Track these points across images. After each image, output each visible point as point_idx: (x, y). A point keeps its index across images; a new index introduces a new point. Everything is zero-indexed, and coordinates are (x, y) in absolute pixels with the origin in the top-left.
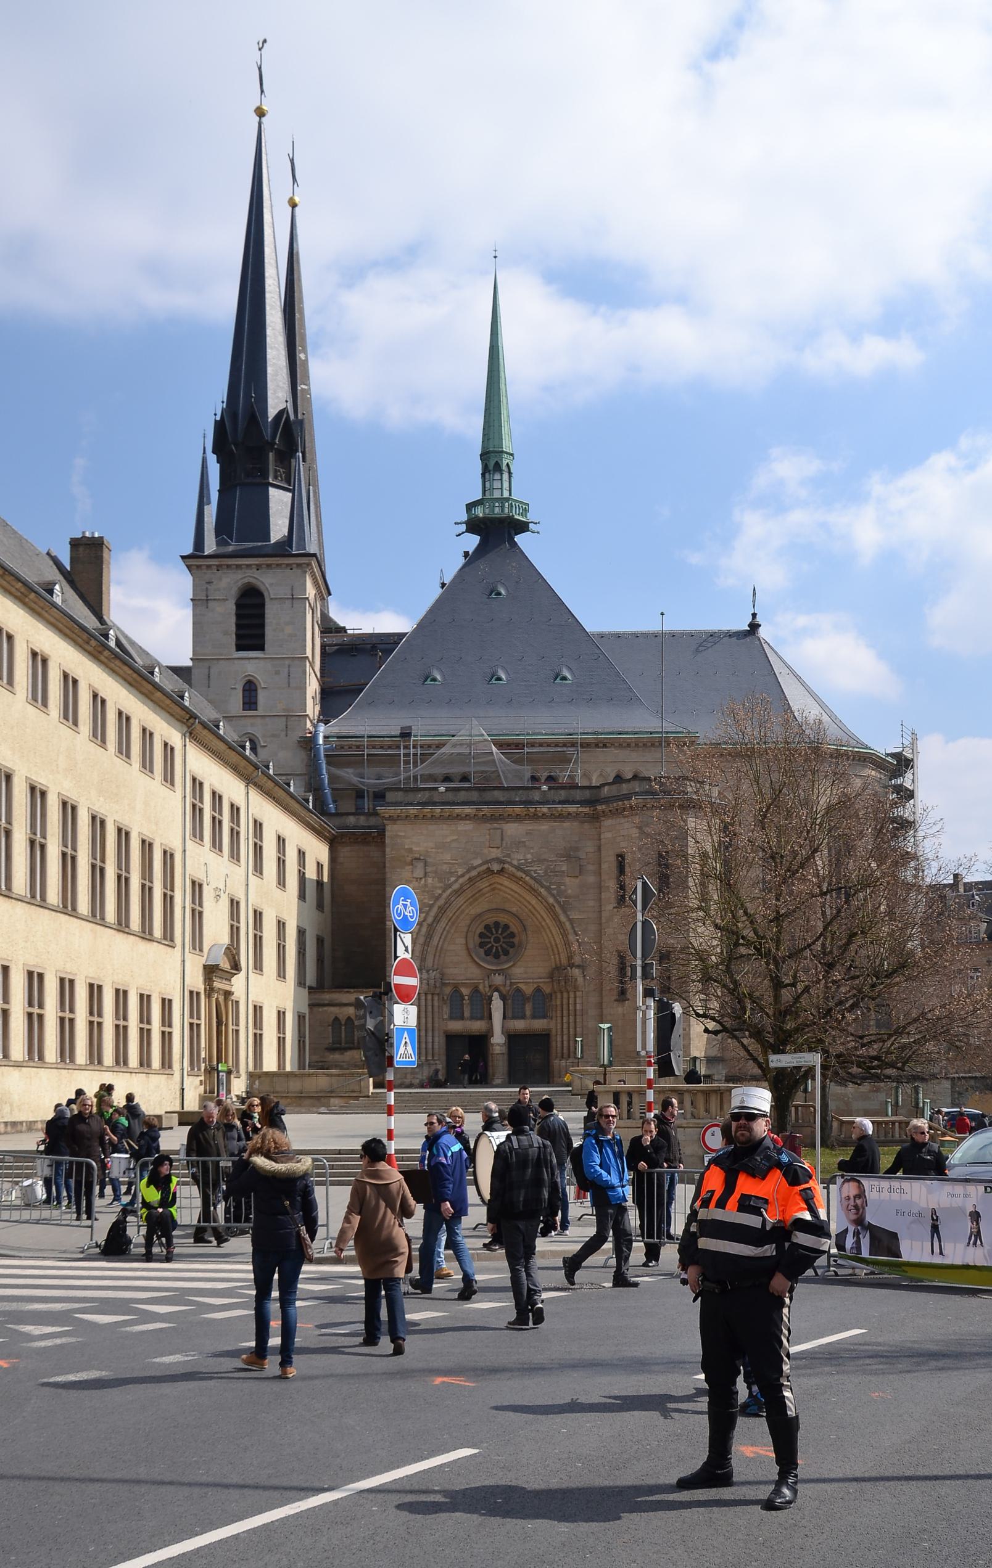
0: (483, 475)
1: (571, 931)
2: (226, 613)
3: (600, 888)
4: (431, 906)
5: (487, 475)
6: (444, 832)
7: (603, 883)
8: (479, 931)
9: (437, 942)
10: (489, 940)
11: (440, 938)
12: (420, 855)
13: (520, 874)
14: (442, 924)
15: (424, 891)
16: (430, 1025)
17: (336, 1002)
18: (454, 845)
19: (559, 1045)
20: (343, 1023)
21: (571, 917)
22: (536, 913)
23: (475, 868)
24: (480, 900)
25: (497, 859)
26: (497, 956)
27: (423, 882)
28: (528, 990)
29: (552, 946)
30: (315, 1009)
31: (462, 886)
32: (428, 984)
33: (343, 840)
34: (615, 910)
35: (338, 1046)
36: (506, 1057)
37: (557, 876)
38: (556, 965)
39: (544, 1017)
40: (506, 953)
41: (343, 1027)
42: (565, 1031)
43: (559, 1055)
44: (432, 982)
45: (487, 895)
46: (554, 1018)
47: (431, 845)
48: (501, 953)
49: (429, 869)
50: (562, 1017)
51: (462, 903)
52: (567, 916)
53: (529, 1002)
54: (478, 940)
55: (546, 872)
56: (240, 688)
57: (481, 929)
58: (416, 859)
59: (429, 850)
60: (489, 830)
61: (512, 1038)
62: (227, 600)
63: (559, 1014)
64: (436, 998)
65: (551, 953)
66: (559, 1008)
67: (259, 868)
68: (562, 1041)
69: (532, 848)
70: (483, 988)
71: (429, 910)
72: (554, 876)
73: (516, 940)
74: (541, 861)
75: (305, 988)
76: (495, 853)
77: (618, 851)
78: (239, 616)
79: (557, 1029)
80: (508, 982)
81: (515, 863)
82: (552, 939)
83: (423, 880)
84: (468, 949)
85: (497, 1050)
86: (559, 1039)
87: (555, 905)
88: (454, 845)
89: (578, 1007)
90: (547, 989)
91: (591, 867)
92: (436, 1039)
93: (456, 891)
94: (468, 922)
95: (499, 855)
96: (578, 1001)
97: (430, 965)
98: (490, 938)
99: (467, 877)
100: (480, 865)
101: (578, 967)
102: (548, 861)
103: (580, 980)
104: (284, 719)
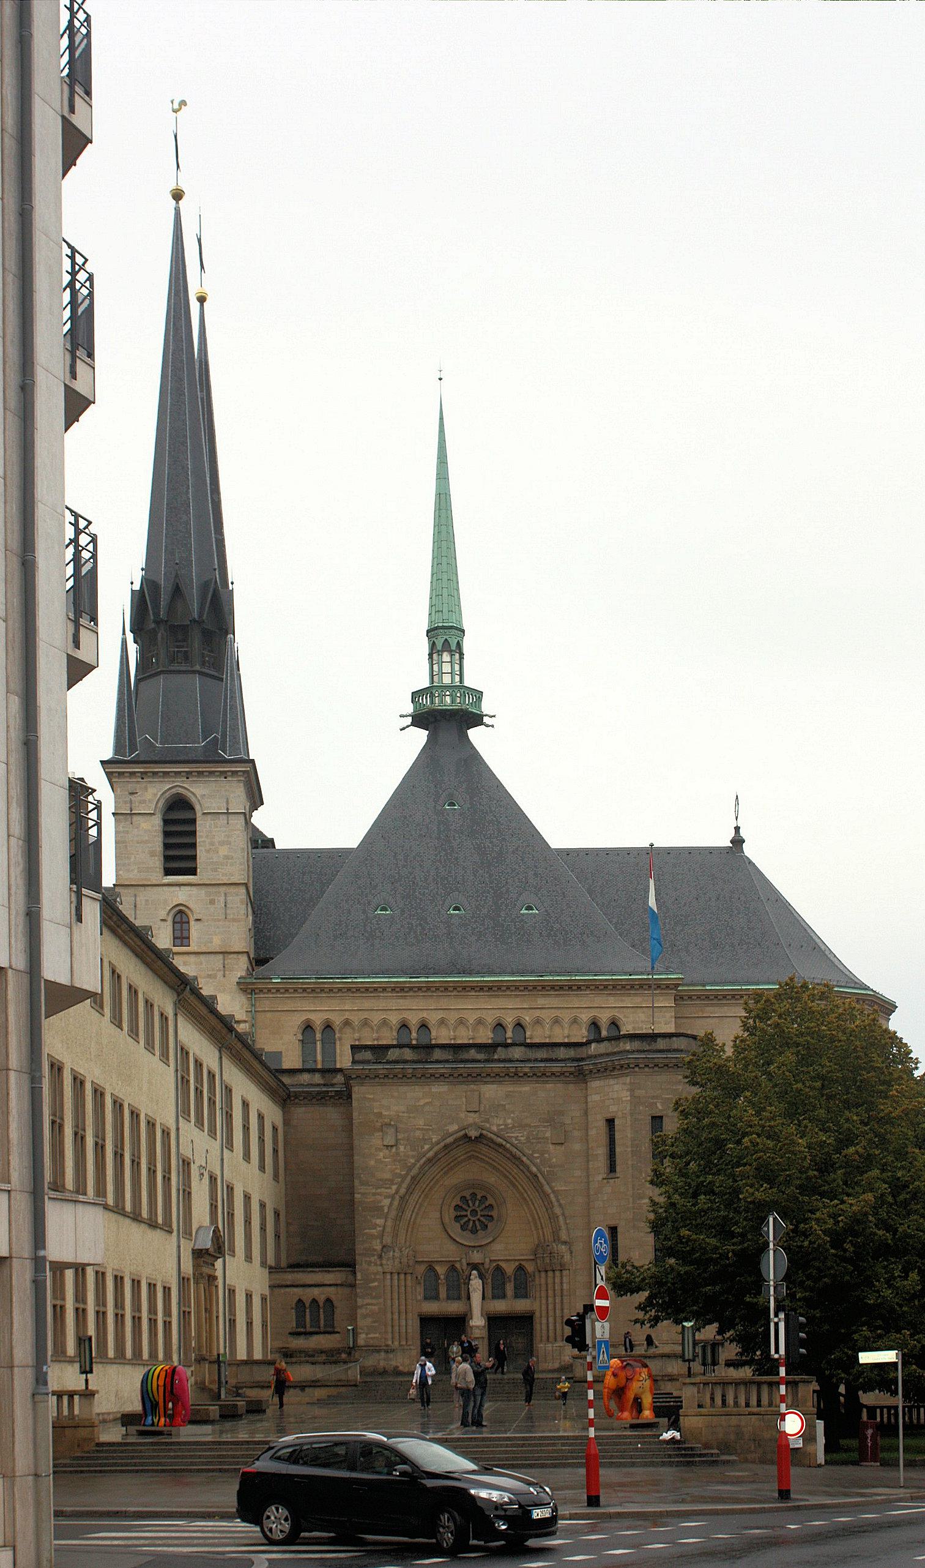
0: (431, 655)
1: (556, 1204)
2: (151, 829)
3: (587, 1156)
4: (404, 1178)
5: (435, 656)
6: (415, 1094)
7: (590, 1152)
8: (454, 1204)
10: (464, 1213)
11: (413, 1212)
12: (391, 1120)
13: (500, 1140)
14: (415, 1196)
16: (403, 1308)
17: (301, 1283)
18: (427, 1108)
19: (544, 1327)
20: (307, 1305)
25: (475, 1124)
26: (474, 1231)
27: (394, 1149)
28: (509, 1269)
29: (534, 1218)
30: (277, 1290)
31: (436, 1154)
32: (401, 1263)
33: (297, 1101)
34: (605, 1181)
35: (302, 1330)
36: (486, 1341)
37: (540, 1143)
38: (539, 1241)
39: (526, 1296)
40: (485, 1227)
41: (308, 1310)
42: (551, 1313)
43: (544, 1338)
44: (405, 1260)
47: (403, 1108)
48: (479, 1227)
49: (400, 1136)
50: (547, 1297)
52: (551, 1188)
53: (510, 1281)
54: (453, 1214)
55: (528, 1138)
56: (170, 919)
57: (457, 1201)
58: (386, 1124)
59: (401, 1114)
60: (466, 1092)
61: (493, 1320)
62: (153, 814)
63: (543, 1294)
64: (409, 1277)
65: (533, 1229)
66: (544, 1288)
67: (229, 1144)
68: (548, 1324)
69: (513, 1112)
70: (462, 1266)
71: (403, 1182)
73: (494, 1213)
74: (522, 1126)
75: (266, 1268)
76: (472, 1118)
77: (609, 1116)
78: (167, 834)
79: (541, 1311)
80: (487, 1260)
81: (495, 1129)
85: (477, 1333)
86: (544, 1321)
87: (539, 1175)
88: (427, 1108)
89: (565, 1286)
90: (530, 1268)
91: (576, 1133)
92: (410, 1322)
93: (430, 1160)
95: (477, 1120)
96: (565, 1280)
97: (403, 1241)
99: (442, 1144)
101: (565, 1243)
102: (530, 1126)
103: (567, 1257)
104: (221, 956)
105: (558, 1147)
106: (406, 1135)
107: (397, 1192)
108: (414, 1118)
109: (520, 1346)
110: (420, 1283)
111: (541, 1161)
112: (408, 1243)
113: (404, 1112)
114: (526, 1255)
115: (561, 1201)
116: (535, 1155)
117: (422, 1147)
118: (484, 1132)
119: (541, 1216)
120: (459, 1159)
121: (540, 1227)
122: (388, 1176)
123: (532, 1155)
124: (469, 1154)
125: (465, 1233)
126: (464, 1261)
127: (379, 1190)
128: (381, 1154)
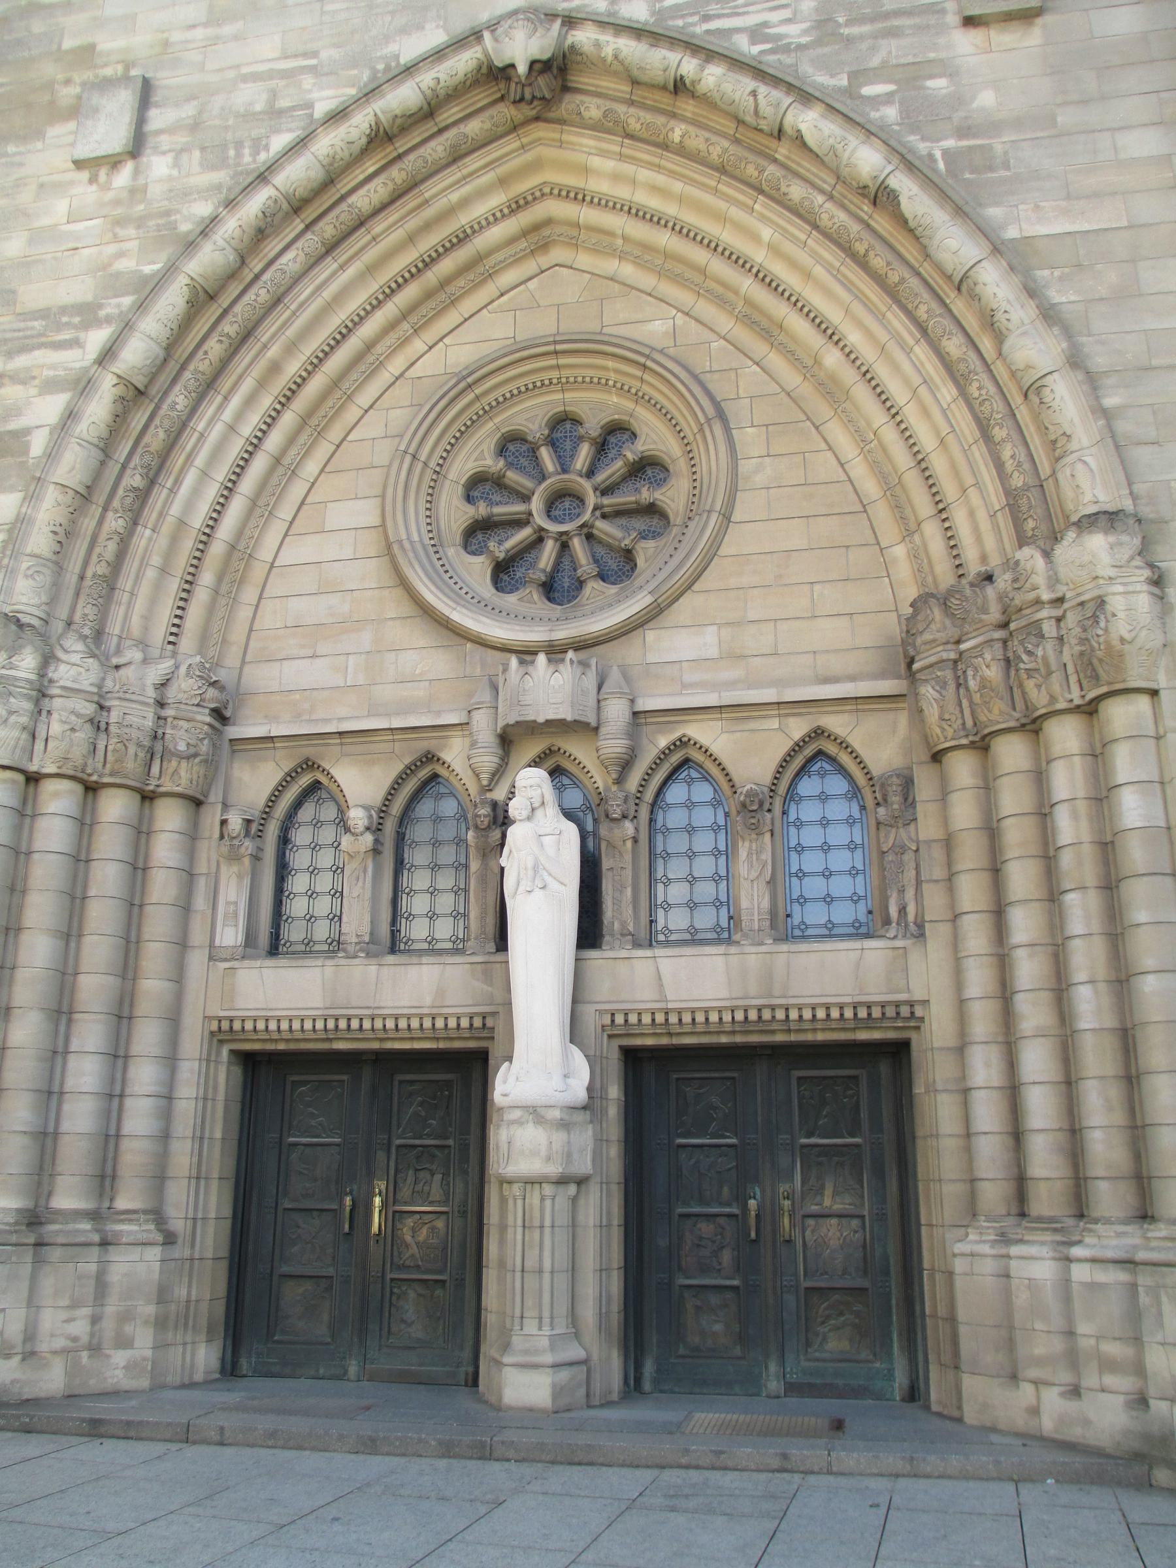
8: (463, 466)
9: (203, 508)
10: (518, 508)
12: (127, 68)
15: (119, 222)
21: (1012, 233)
22: (780, 309)
23: (409, 70)
24: (468, 306)
27: (123, 177)
45: (508, 278)
46: (937, 937)
49: (157, 119)
51: (353, 305)
52: (984, 232)
59: (176, 36)
66: (971, 854)
71: (141, 306)
72: (875, 36)
79: (961, 1004)
81: (637, 11)
82: (890, 435)
83: (129, 166)
84: (388, 551)
87: (904, 185)
94: (399, 417)
98: (526, 498)
99: (360, 124)
100: (438, 55)
105: (1004, 38)
106: (189, 111)
107: (107, 355)
108: (236, 38)
109: (832, 1233)
110: (234, 857)
111: (905, 113)
112: (187, 643)
113: (194, 26)
114: (852, 678)
115: (1056, 296)
116: (867, 91)
117: (258, 145)
118: (584, 37)
119: (927, 440)
120: (482, 242)
121: (923, 505)
122: (77, 290)
123: (850, 92)
124: (525, 218)
125: (511, 599)
126: (484, 728)
127: (22, 361)
128: (61, 207)
